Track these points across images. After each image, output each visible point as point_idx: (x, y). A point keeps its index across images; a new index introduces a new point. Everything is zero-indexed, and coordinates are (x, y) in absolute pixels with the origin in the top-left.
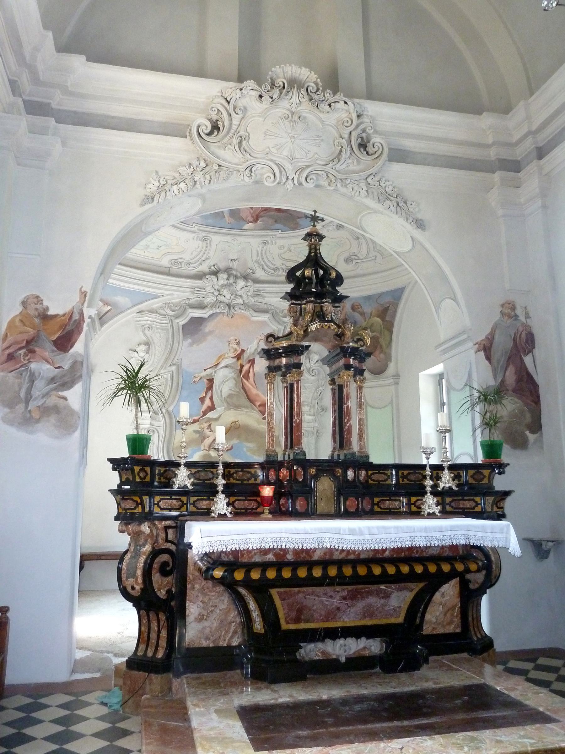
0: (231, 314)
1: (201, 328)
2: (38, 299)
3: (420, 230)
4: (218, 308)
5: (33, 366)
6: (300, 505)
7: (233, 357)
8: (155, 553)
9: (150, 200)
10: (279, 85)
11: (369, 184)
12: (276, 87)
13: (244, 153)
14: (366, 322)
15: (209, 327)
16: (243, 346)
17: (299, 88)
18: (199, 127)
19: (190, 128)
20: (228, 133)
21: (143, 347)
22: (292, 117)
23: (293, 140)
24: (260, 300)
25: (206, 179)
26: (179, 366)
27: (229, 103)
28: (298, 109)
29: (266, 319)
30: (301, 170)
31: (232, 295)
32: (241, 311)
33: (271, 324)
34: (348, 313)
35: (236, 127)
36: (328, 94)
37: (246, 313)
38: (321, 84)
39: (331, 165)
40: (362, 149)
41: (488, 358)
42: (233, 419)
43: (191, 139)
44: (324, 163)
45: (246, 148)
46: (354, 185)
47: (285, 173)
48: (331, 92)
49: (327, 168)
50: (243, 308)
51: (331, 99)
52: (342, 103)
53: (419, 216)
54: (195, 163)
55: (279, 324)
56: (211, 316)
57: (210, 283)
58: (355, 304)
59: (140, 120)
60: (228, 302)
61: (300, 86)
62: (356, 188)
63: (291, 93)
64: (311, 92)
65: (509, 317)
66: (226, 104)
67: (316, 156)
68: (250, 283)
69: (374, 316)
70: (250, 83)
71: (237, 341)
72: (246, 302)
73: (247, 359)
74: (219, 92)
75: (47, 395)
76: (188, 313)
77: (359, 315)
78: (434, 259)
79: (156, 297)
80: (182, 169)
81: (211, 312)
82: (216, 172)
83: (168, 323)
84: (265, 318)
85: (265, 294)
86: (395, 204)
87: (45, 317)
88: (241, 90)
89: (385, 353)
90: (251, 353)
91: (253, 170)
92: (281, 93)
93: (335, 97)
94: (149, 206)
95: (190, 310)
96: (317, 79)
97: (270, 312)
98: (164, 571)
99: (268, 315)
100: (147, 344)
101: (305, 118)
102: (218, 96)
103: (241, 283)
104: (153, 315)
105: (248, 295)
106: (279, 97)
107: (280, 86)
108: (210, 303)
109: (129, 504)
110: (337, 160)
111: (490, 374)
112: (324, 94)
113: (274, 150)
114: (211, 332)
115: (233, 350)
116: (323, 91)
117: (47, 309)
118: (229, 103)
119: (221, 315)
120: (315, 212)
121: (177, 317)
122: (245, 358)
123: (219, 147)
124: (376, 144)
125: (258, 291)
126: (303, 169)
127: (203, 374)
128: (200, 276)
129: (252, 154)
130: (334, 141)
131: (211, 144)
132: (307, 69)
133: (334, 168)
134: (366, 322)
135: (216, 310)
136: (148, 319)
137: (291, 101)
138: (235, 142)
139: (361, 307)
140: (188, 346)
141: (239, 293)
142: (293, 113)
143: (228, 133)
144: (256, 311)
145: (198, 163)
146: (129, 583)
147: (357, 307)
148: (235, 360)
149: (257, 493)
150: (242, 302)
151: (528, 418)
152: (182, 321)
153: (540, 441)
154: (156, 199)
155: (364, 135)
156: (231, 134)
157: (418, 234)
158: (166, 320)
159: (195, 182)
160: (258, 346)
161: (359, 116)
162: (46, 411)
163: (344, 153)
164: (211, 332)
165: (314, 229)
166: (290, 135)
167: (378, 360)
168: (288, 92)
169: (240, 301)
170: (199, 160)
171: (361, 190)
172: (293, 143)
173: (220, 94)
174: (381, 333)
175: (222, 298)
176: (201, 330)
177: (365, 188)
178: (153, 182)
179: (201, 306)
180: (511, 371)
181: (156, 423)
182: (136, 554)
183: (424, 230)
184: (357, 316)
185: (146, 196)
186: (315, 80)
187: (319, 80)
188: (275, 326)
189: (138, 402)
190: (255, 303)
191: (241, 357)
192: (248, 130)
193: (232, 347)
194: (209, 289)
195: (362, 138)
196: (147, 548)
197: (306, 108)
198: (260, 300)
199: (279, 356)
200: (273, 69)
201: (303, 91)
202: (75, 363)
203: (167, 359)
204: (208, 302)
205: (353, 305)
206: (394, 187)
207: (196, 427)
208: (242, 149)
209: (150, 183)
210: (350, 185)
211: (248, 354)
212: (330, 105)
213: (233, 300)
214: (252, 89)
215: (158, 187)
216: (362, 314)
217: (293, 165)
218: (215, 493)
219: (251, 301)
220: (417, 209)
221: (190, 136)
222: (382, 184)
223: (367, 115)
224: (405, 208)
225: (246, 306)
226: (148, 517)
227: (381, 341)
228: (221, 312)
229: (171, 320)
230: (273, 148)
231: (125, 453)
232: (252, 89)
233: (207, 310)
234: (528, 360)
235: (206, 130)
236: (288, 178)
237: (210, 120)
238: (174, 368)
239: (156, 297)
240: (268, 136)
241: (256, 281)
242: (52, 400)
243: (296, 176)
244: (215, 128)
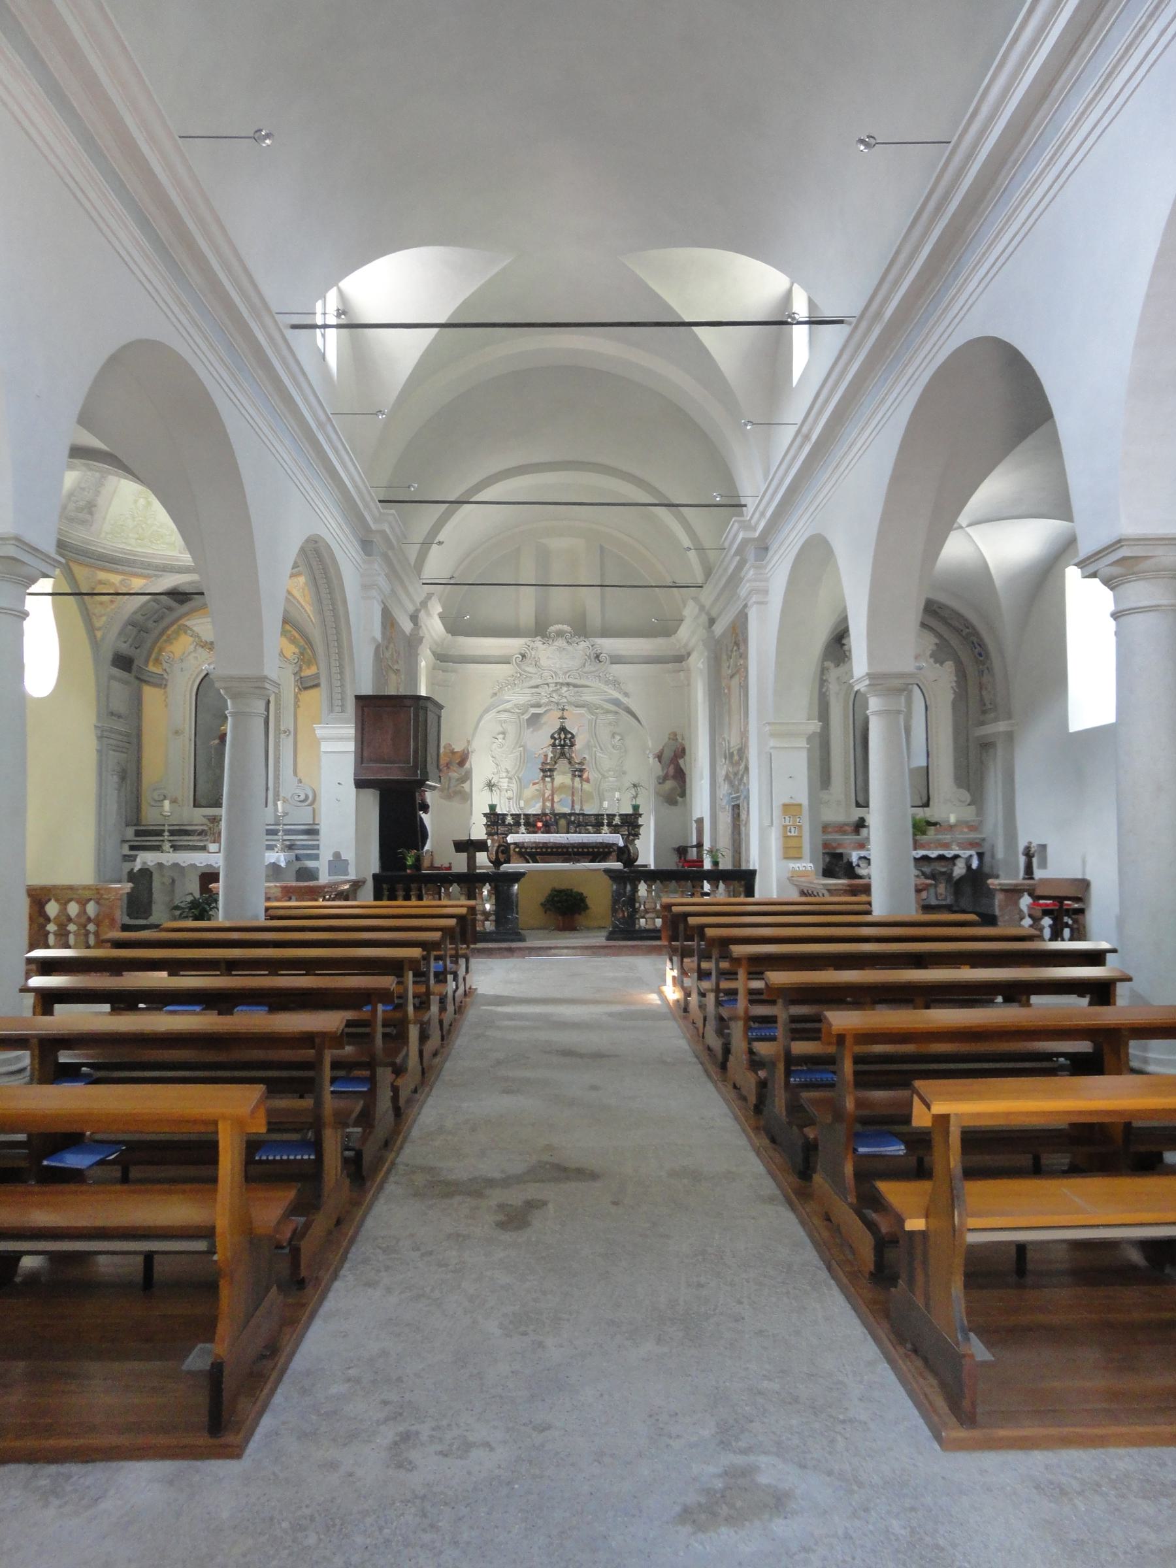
2: (450, 745)
5: (450, 774)
6: (553, 828)
8: (499, 847)
15: (544, 719)
21: (501, 736)
26: (524, 746)
41: (660, 762)
42: (561, 782)
51: (577, 641)
54: (515, 675)
56: (546, 711)
57: (544, 691)
65: (673, 740)
68: (571, 688)
70: (539, 638)
75: (456, 786)
79: (508, 701)
84: (582, 711)
87: (453, 753)
94: (493, 699)
98: (503, 852)
100: (504, 733)
103: (565, 689)
104: (506, 713)
109: (489, 829)
111: (660, 769)
114: (545, 724)
117: (453, 749)
121: (523, 714)
125: (578, 692)
126: (566, 673)
127: (541, 752)
128: (537, 687)
135: (547, 708)
136: (504, 716)
138: (534, 663)
144: (576, 707)
146: (490, 856)
149: (536, 825)
151: (679, 790)
152: (526, 717)
153: (684, 803)
158: (515, 716)
161: (592, 646)
162: (457, 793)
175: (553, 699)
179: (538, 705)
180: (672, 767)
181: (511, 785)
182: (493, 846)
183: (629, 697)
189: (492, 791)
194: (543, 694)
196: (497, 844)
197: (565, 644)
199: (547, 771)
202: (466, 772)
203: (517, 743)
207: (536, 787)
218: (520, 825)
219: (573, 699)
225: (570, 703)
226: (497, 833)
231: (488, 811)
234: (681, 762)
237: (521, 654)
238: (521, 749)
239: (508, 701)
241: (575, 686)
242: (458, 788)
244: (524, 656)
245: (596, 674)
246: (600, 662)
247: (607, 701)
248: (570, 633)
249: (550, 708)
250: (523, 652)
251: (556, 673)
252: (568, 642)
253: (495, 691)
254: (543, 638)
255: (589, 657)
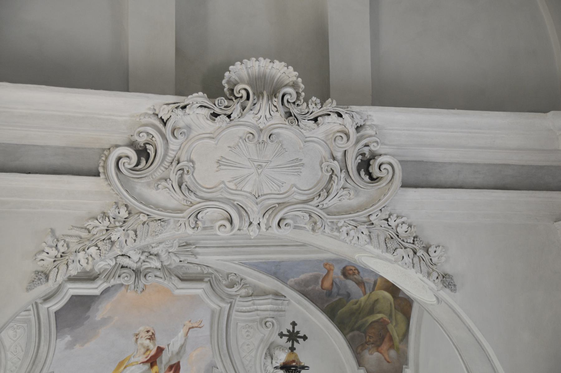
0: (141, 286)
1: (87, 314)
3: (447, 290)
4: (119, 276)
7: (143, 363)
9: (43, 277)
10: (239, 95)
11: (373, 224)
12: (236, 98)
13: (186, 193)
14: (368, 295)
16: (161, 342)
17: (270, 98)
18: (119, 159)
19: (104, 158)
20: (163, 160)
22: (259, 136)
23: (259, 171)
24: (191, 259)
25: (128, 236)
27: (165, 124)
28: (270, 123)
29: (199, 292)
30: (270, 212)
31: (143, 252)
32: (157, 279)
33: (208, 301)
34: (337, 280)
35: (174, 153)
36: (314, 105)
37: (166, 283)
38: (302, 86)
39: (315, 202)
40: (362, 173)
43: (107, 178)
44: (305, 198)
45: (189, 184)
46: (350, 227)
47: (247, 219)
48: (318, 101)
49: (309, 207)
50: (161, 275)
51: (317, 112)
52: (334, 116)
53: (448, 269)
55: (223, 300)
58: (348, 268)
59: (24, 145)
60: (134, 266)
61: (273, 94)
62: (352, 233)
63: (257, 106)
64: (288, 102)
66: (161, 126)
67: (294, 189)
69: (381, 289)
71: (150, 333)
72: (166, 263)
73: (167, 364)
74: (150, 109)
76: (65, 290)
77: (354, 283)
78: (470, 330)
80: (92, 224)
81: (105, 286)
82: (144, 224)
83: (29, 310)
85: (198, 250)
86: (411, 253)
88: (184, 107)
89: (398, 350)
90: (175, 353)
91: (200, 216)
92: (244, 108)
93: (324, 108)
95: (70, 285)
96: (298, 77)
97: (206, 279)
99: (205, 285)
101: (278, 135)
102: (149, 115)
105: (169, 253)
106: (241, 116)
107: (241, 97)
108: (105, 270)
110: (324, 194)
112: (308, 105)
113: (232, 186)
114: (105, 321)
115: (143, 350)
116: (306, 100)
118: (165, 124)
119: (123, 288)
120: (294, 324)
122: (164, 362)
123: (149, 184)
124: (383, 167)
129: (198, 193)
130: (321, 163)
131: (136, 180)
132: (283, 63)
133: (320, 206)
134: (368, 295)
137: (259, 115)
138: (174, 178)
139: (359, 273)
140: (66, 348)
141: (154, 251)
142: (261, 130)
143: (163, 160)
144: (182, 280)
145: (117, 211)
147: (351, 272)
148: (147, 366)
150: (158, 265)
154: (52, 276)
155: (366, 150)
156: (166, 164)
157: (445, 294)
159: (113, 243)
160: (185, 340)
161: (358, 128)
163: (336, 182)
164: (105, 321)
165: (292, 358)
166: (256, 164)
167: (385, 359)
168: (255, 104)
169: (155, 263)
170: (118, 207)
171: (361, 236)
172: (259, 175)
173: (151, 112)
174: (390, 316)
175: (125, 261)
176: (88, 317)
177: (366, 232)
178: (47, 250)
184: (351, 285)
185: (37, 272)
186: (295, 79)
187: (300, 80)
188: (214, 303)
190: (181, 264)
191: (158, 360)
192: (193, 157)
193: (142, 344)
195: (363, 155)
198: (191, 259)
200: (231, 67)
201: (277, 101)
204: (101, 268)
205: (344, 268)
206: (410, 226)
208: (183, 187)
209: (43, 251)
210: (344, 229)
211: (169, 355)
212: (315, 120)
213: (144, 261)
214: (201, 106)
215: (56, 257)
216: (360, 283)
217: (259, 205)
220: (443, 259)
221: (104, 173)
222: (391, 222)
223: (371, 126)
224: (427, 258)
225: (167, 271)
227: (391, 327)
228: (122, 285)
229: (36, 303)
230: (229, 182)
232: (201, 106)
233: (99, 282)
235: (129, 164)
236: (251, 223)
240: (222, 167)
243: (263, 222)
245: (362, 216)
246: (372, 179)
247: (256, 266)
248: (294, 85)
249: (118, 281)
250: (141, 140)
251: (240, 209)
252: (289, 114)
253: (39, 266)
254: (212, 96)
255: (345, 167)
